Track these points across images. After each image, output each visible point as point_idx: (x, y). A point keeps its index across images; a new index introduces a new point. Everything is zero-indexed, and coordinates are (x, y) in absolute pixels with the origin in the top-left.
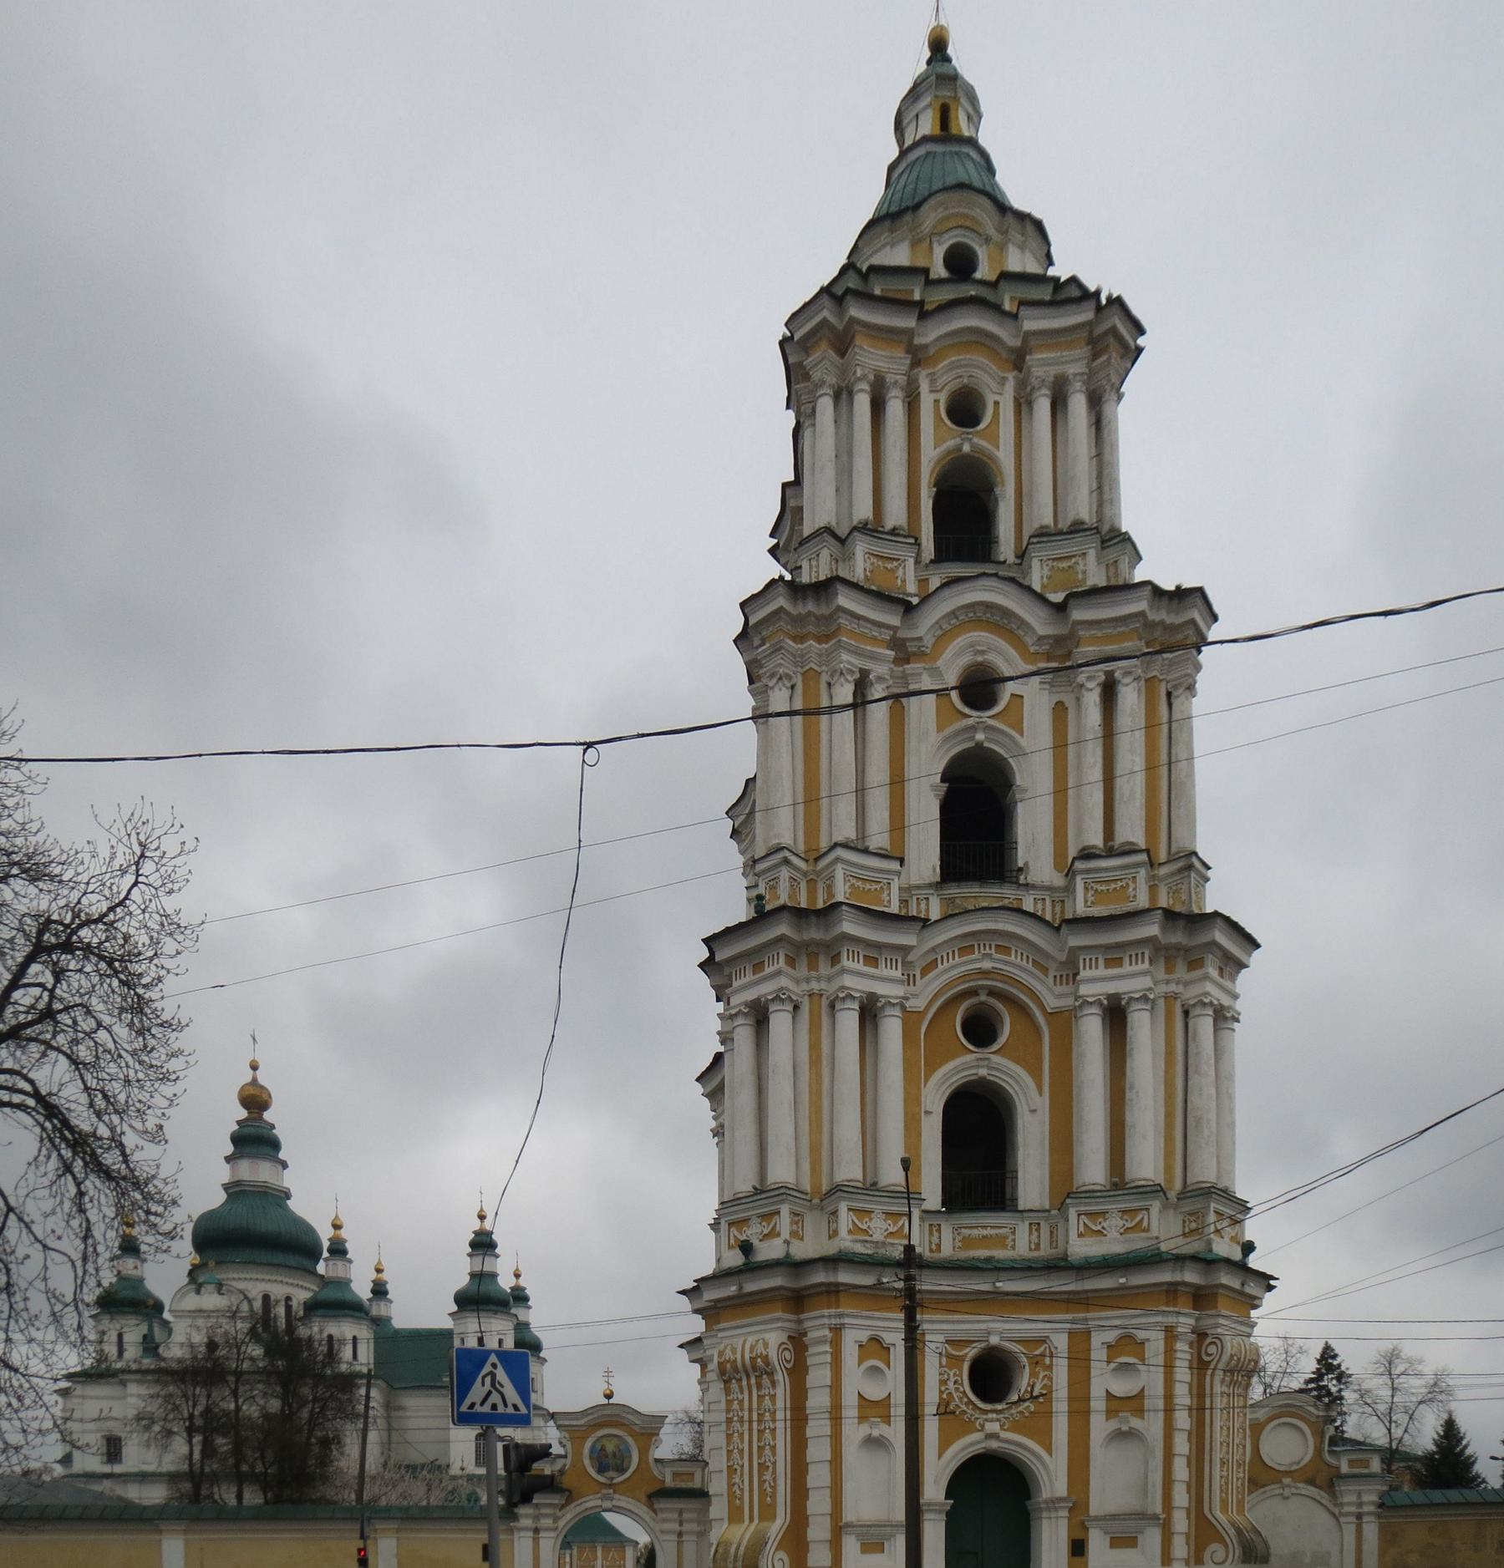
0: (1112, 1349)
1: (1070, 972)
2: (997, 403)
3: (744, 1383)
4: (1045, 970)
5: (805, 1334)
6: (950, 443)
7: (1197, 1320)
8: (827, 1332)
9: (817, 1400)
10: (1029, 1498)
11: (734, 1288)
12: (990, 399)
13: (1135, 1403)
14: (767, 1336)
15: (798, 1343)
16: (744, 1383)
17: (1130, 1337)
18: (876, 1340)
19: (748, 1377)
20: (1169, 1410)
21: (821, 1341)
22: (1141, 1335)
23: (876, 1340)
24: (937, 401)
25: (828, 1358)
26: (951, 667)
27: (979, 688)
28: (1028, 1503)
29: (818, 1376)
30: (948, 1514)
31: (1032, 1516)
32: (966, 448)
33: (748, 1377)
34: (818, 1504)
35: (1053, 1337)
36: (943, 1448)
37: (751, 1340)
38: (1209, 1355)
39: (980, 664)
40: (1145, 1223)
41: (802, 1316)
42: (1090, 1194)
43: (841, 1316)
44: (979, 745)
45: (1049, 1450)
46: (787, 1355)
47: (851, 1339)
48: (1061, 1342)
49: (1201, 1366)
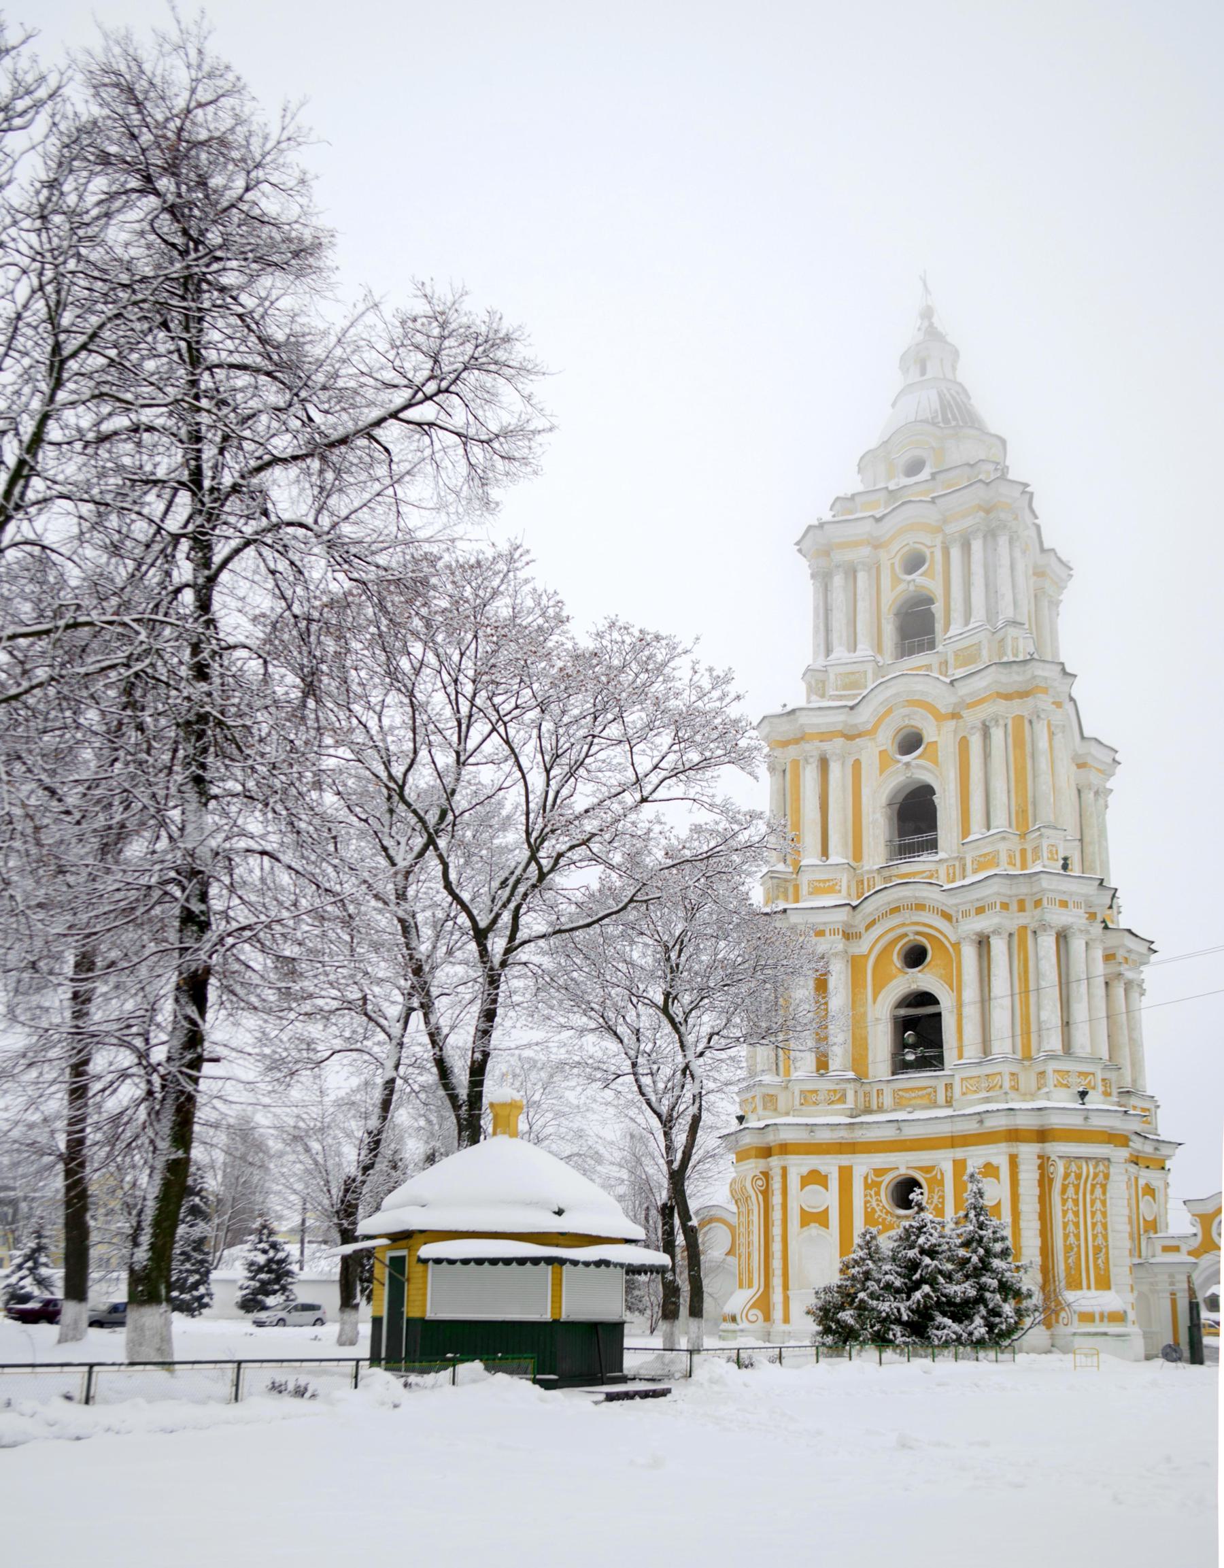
6: (902, 586)
12: (927, 552)
17: (988, 1165)
22: (995, 1161)
24: (893, 564)
27: (911, 743)
49: (1045, 1182)
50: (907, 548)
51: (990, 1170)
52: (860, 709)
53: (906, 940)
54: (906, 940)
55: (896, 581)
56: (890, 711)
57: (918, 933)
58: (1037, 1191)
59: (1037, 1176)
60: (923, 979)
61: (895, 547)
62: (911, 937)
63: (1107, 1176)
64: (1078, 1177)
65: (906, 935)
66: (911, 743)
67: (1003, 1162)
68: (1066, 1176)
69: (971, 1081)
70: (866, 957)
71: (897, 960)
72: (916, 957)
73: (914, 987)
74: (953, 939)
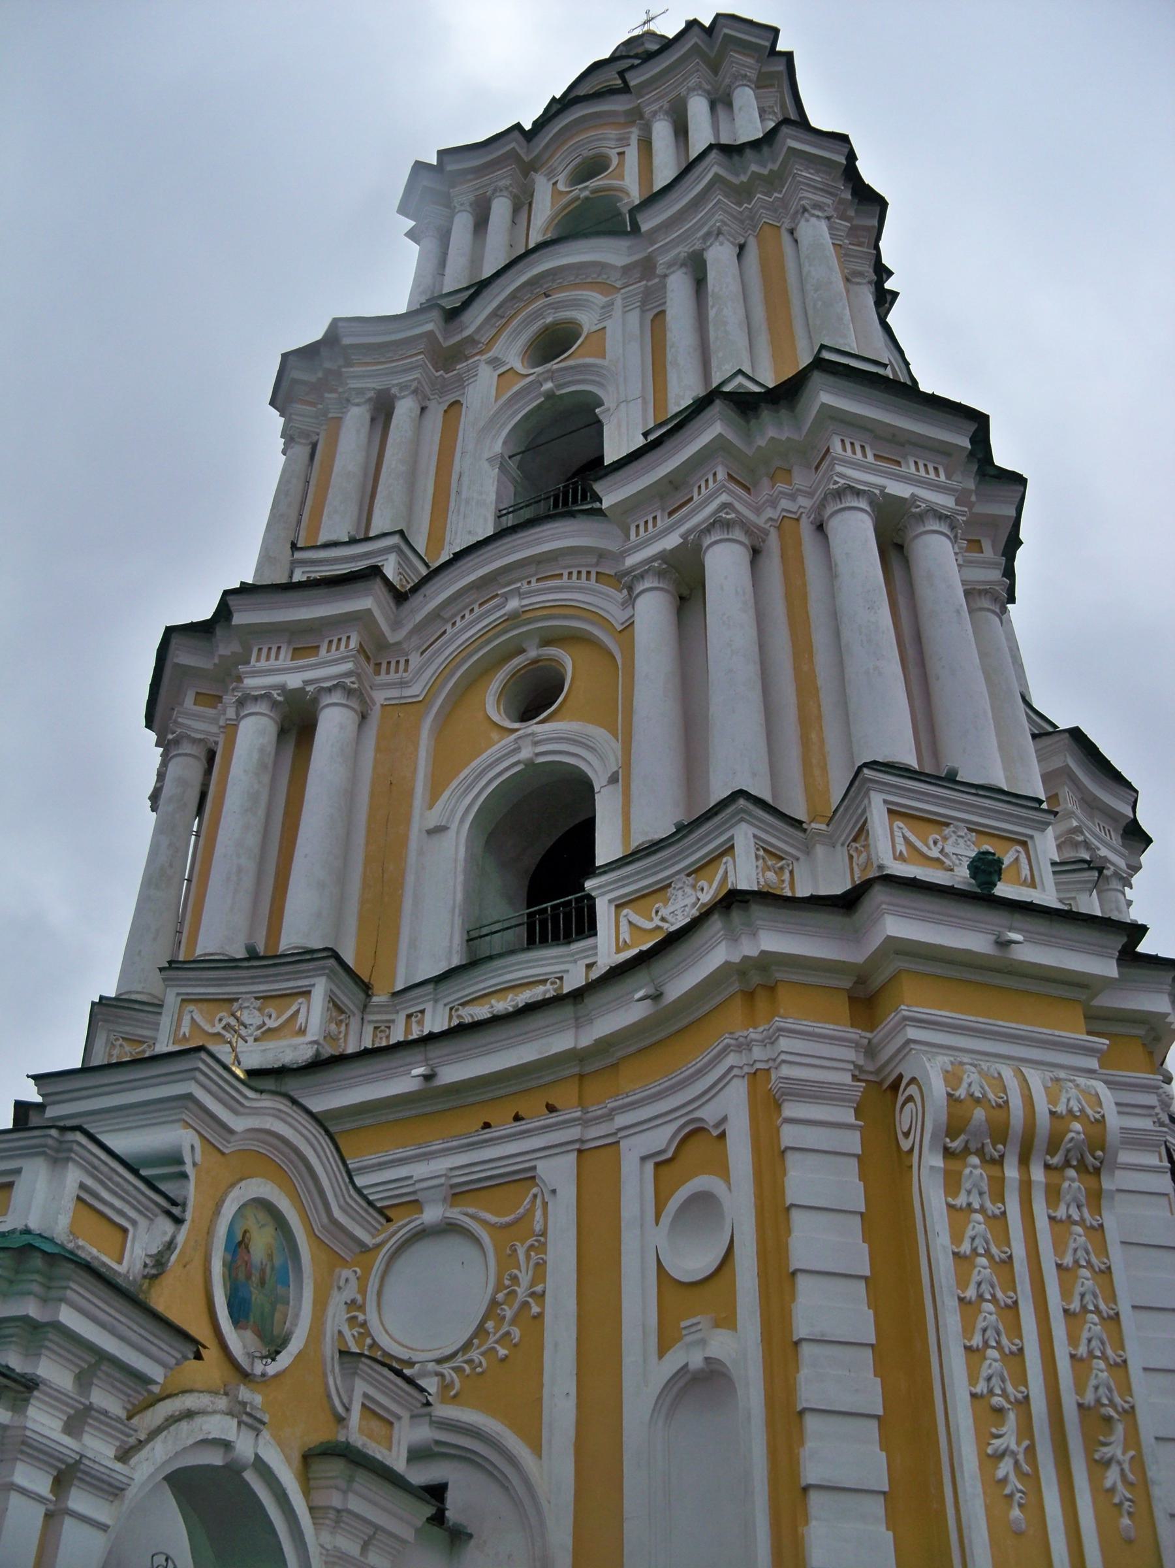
0: (664, 1166)
2: (621, 154)
7: (870, 1051)
12: (613, 153)
20: (779, 1279)
35: (544, 1168)
39: (555, 323)
44: (550, 396)
45: (537, 1448)
48: (559, 1173)
52: (467, 316)
53: (517, 662)
54: (517, 662)
55: (556, 193)
58: (850, 1190)
59: (853, 1142)
60: (553, 738)
62: (533, 653)
63: (1097, 1138)
64: (1000, 1133)
67: (733, 1107)
68: (953, 1128)
70: (422, 704)
71: (491, 703)
73: (526, 753)
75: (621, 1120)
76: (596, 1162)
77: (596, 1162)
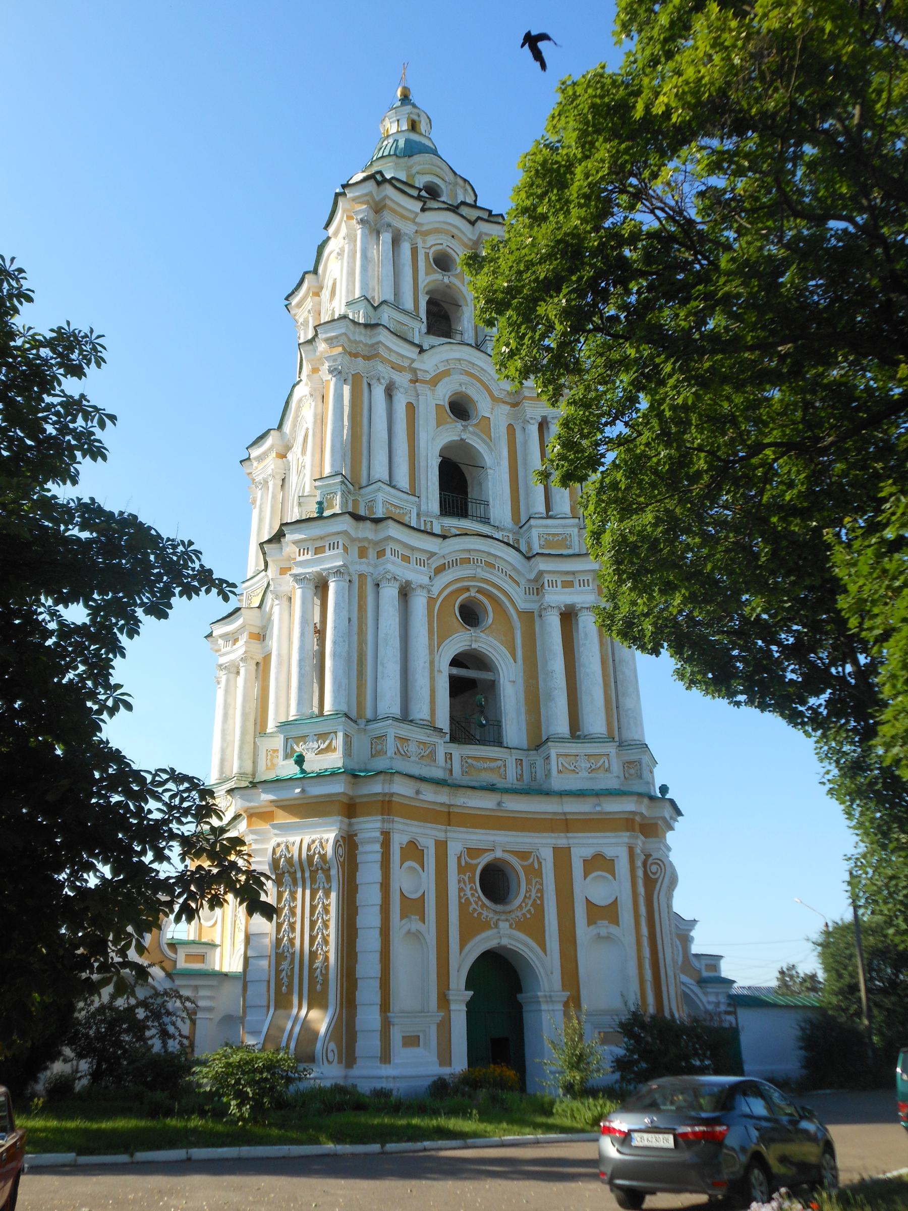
1: (537, 587)
3: (299, 875)
4: (518, 584)
5: (356, 835)
8: (378, 834)
9: (369, 895)
10: (520, 990)
11: (298, 790)
13: (610, 912)
14: (325, 836)
15: (349, 843)
16: (299, 875)
18: (412, 844)
19: (303, 871)
21: (372, 841)
22: (609, 852)
23: (412, 844)
25: (378, 857)
26: (444, 392)
27: (460, 409)
28: (519, 996)
29: (369, 874)
30: (468, 1005)
31: (525, 1008)
32: (446, 280)
33: (303, 871)
34: (368, 993)
36: (463, 943)
37: (307, 840)
38: (655, 874)
40: (607, 765)
41: (354, 820)
42: (562, 740)
43: (389, 822)
46: (340, 851)
47: (398, 840)
50: (440, 247)
51: (599, 863)
53: (466, 595)
54: (466, 595)
56: (446, 373)
57: (480, 591)
61: (431, 240)
62: (473, 593)
65: (467, 589)
66: (460, 409)
69: (568, 759)
72: (470, 615)
73: (474, 646)
74: (522, 606)
75: (571, 841)
76: (562, 856)
77: (562, 856)
